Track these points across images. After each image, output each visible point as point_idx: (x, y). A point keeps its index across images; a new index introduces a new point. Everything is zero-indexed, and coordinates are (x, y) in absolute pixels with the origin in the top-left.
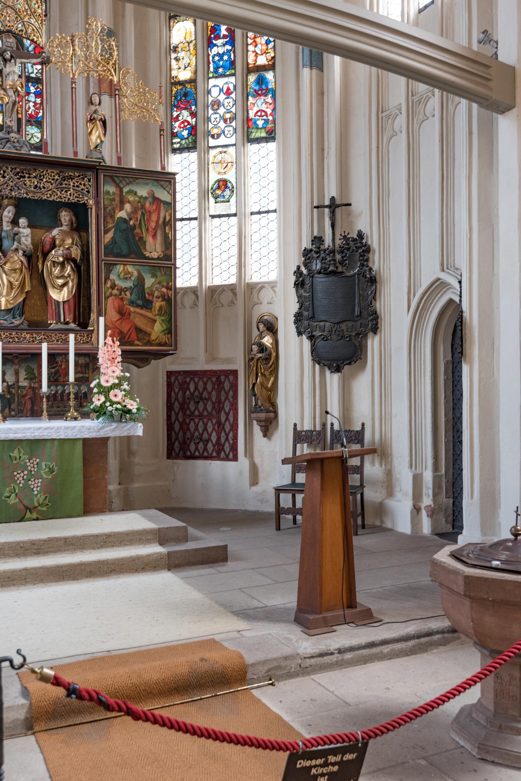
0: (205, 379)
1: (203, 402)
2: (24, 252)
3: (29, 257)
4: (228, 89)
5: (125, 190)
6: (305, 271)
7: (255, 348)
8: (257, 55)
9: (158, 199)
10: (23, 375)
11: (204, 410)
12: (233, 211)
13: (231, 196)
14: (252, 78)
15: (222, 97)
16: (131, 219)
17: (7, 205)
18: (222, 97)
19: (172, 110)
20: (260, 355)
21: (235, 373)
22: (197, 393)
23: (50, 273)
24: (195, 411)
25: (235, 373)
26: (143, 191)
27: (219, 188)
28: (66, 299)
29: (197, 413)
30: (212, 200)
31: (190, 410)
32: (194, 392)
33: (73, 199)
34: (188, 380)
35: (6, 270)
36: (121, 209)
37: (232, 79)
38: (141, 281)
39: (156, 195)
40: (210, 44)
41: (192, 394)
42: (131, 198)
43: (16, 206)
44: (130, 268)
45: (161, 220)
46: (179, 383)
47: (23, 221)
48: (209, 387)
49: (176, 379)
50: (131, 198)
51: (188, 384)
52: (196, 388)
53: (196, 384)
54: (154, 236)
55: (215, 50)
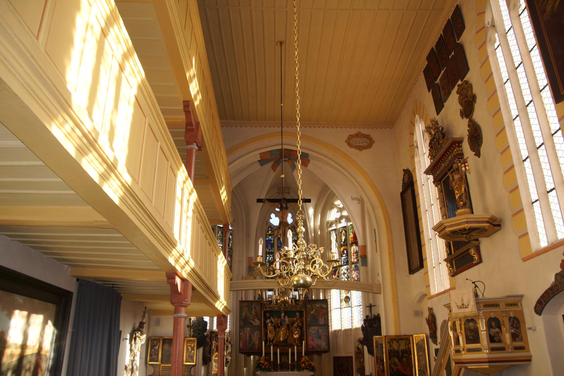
2: (287, 325)
3: (288, 326)
4: (347, 269)
5: (313, 306)
6: (364, 326)
7: (357, 349)
8: (354, 259)
9: (322, 307)
10: (286, 359)
12: (350, 306)
13: (349, 301)
14: (353, 266)
15: (346, 272)
16: (315, 314)
17: (282, 313)
18: (346, 272)
19: (333, 276)
20: (357, 351)
21: (352, 357)
23: (293, 330)
25: (352, 357)
26: (318, 305)
27: (345, 299)
28: (298, 337)
30: (344, 302)
33: (299, 310)
35: (282, 330)
36: (312, 311)
37: (348, 266)
38: (318, 331)
39: (322, 306)
40: (342, 256)
42: (315, 308)
43: (284, 313)
44: (315, 327)
45: (323, 313)
47: (286, 317)
50: (315, 308)
54: (322, 318)
55: (343, 258)
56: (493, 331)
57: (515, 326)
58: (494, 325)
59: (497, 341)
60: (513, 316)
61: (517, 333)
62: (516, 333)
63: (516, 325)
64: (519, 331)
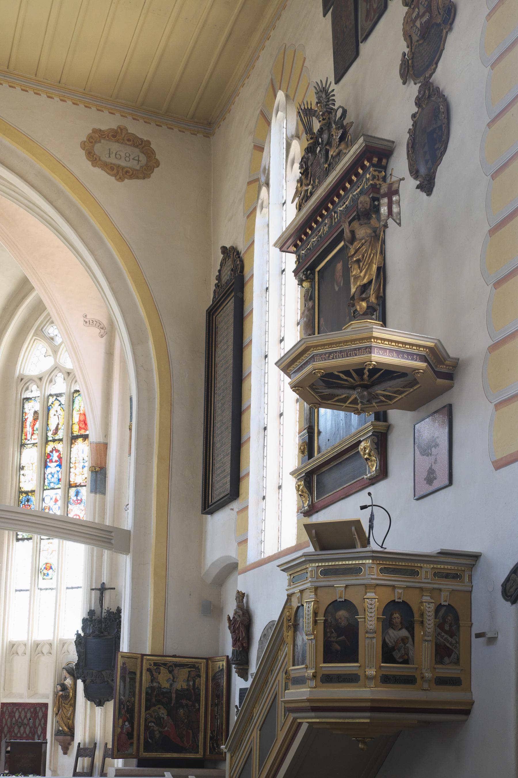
0: (26, 710)
1: (24, 727)
11: (23, 733)
22: (20, 720)
24: (18, 733)
29: (19, 735)
31: (14, 733)
32: (18, 719)
34: (15, 709)
41: (17, 721)
46: (9, 711)
48: (29, 715)
49: (7, 709)
51: (15, 713)
52: (20, 716)
53: (20, 713)
56: (394, 635)
57: (447, 628)
58: (398, 620)
59: (400, 660)
60: (446, 604)
61: (450, 647)
62: (448, 645)
63: (450, 626)
64: (454, 642)
